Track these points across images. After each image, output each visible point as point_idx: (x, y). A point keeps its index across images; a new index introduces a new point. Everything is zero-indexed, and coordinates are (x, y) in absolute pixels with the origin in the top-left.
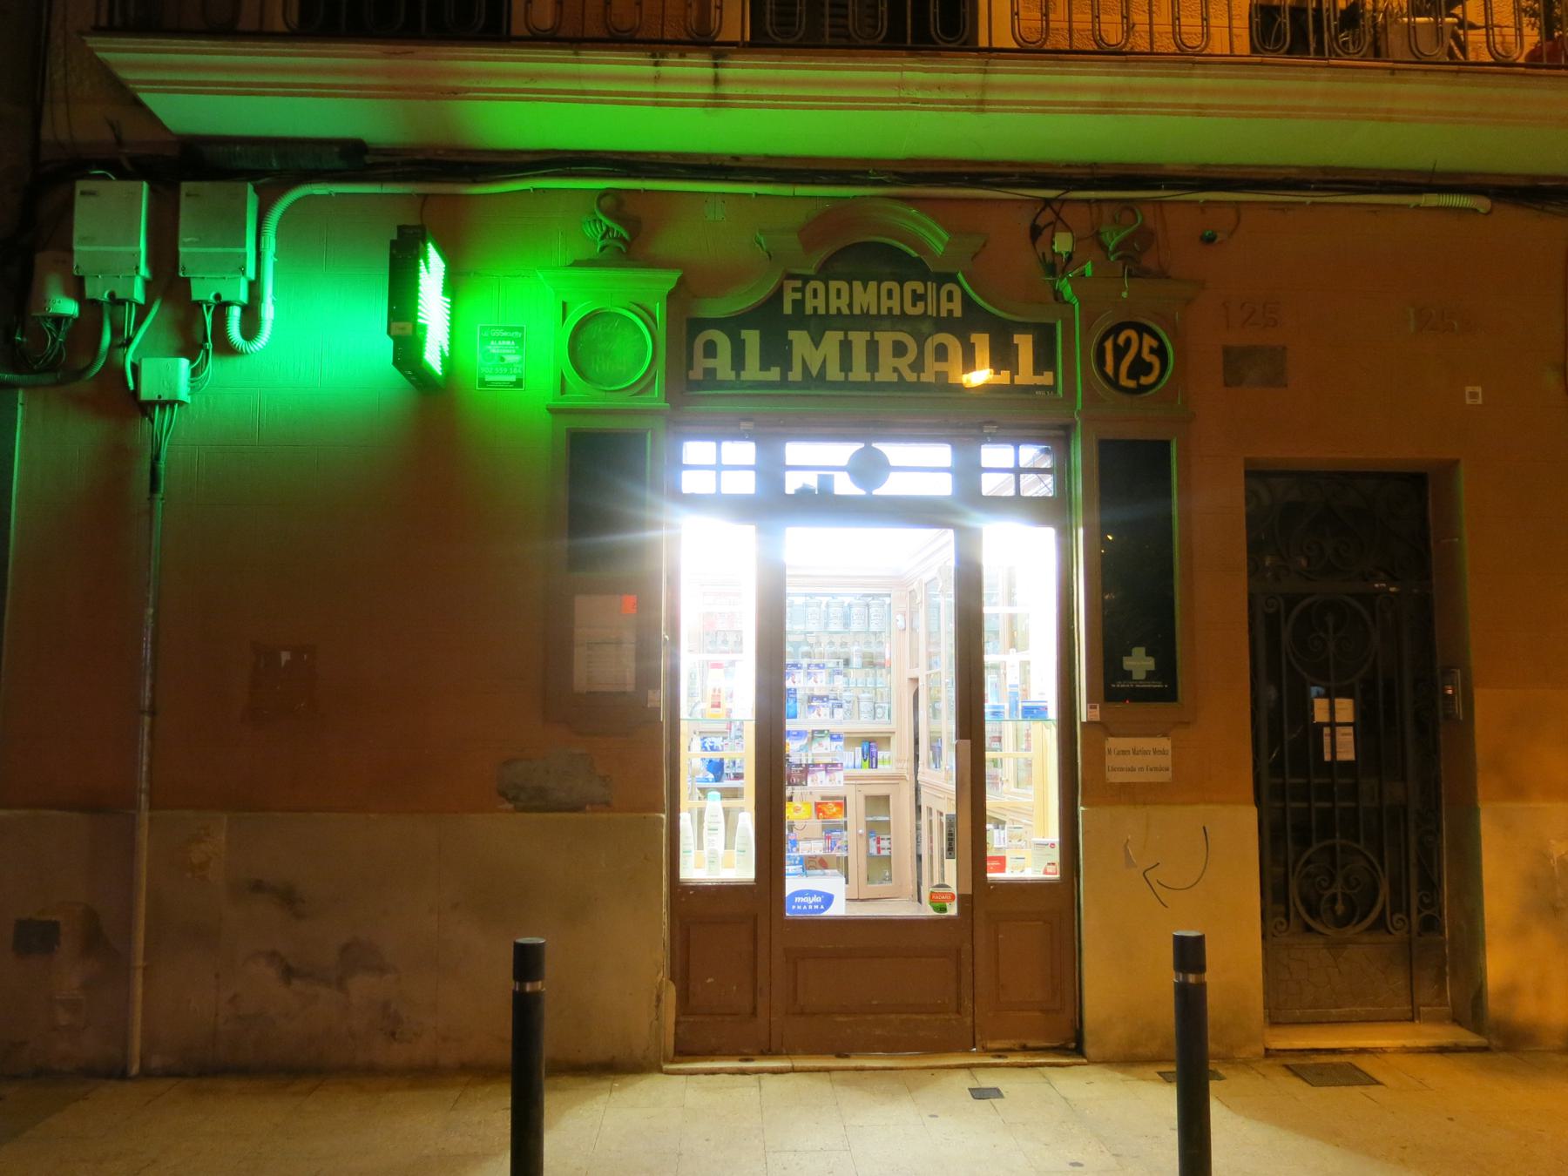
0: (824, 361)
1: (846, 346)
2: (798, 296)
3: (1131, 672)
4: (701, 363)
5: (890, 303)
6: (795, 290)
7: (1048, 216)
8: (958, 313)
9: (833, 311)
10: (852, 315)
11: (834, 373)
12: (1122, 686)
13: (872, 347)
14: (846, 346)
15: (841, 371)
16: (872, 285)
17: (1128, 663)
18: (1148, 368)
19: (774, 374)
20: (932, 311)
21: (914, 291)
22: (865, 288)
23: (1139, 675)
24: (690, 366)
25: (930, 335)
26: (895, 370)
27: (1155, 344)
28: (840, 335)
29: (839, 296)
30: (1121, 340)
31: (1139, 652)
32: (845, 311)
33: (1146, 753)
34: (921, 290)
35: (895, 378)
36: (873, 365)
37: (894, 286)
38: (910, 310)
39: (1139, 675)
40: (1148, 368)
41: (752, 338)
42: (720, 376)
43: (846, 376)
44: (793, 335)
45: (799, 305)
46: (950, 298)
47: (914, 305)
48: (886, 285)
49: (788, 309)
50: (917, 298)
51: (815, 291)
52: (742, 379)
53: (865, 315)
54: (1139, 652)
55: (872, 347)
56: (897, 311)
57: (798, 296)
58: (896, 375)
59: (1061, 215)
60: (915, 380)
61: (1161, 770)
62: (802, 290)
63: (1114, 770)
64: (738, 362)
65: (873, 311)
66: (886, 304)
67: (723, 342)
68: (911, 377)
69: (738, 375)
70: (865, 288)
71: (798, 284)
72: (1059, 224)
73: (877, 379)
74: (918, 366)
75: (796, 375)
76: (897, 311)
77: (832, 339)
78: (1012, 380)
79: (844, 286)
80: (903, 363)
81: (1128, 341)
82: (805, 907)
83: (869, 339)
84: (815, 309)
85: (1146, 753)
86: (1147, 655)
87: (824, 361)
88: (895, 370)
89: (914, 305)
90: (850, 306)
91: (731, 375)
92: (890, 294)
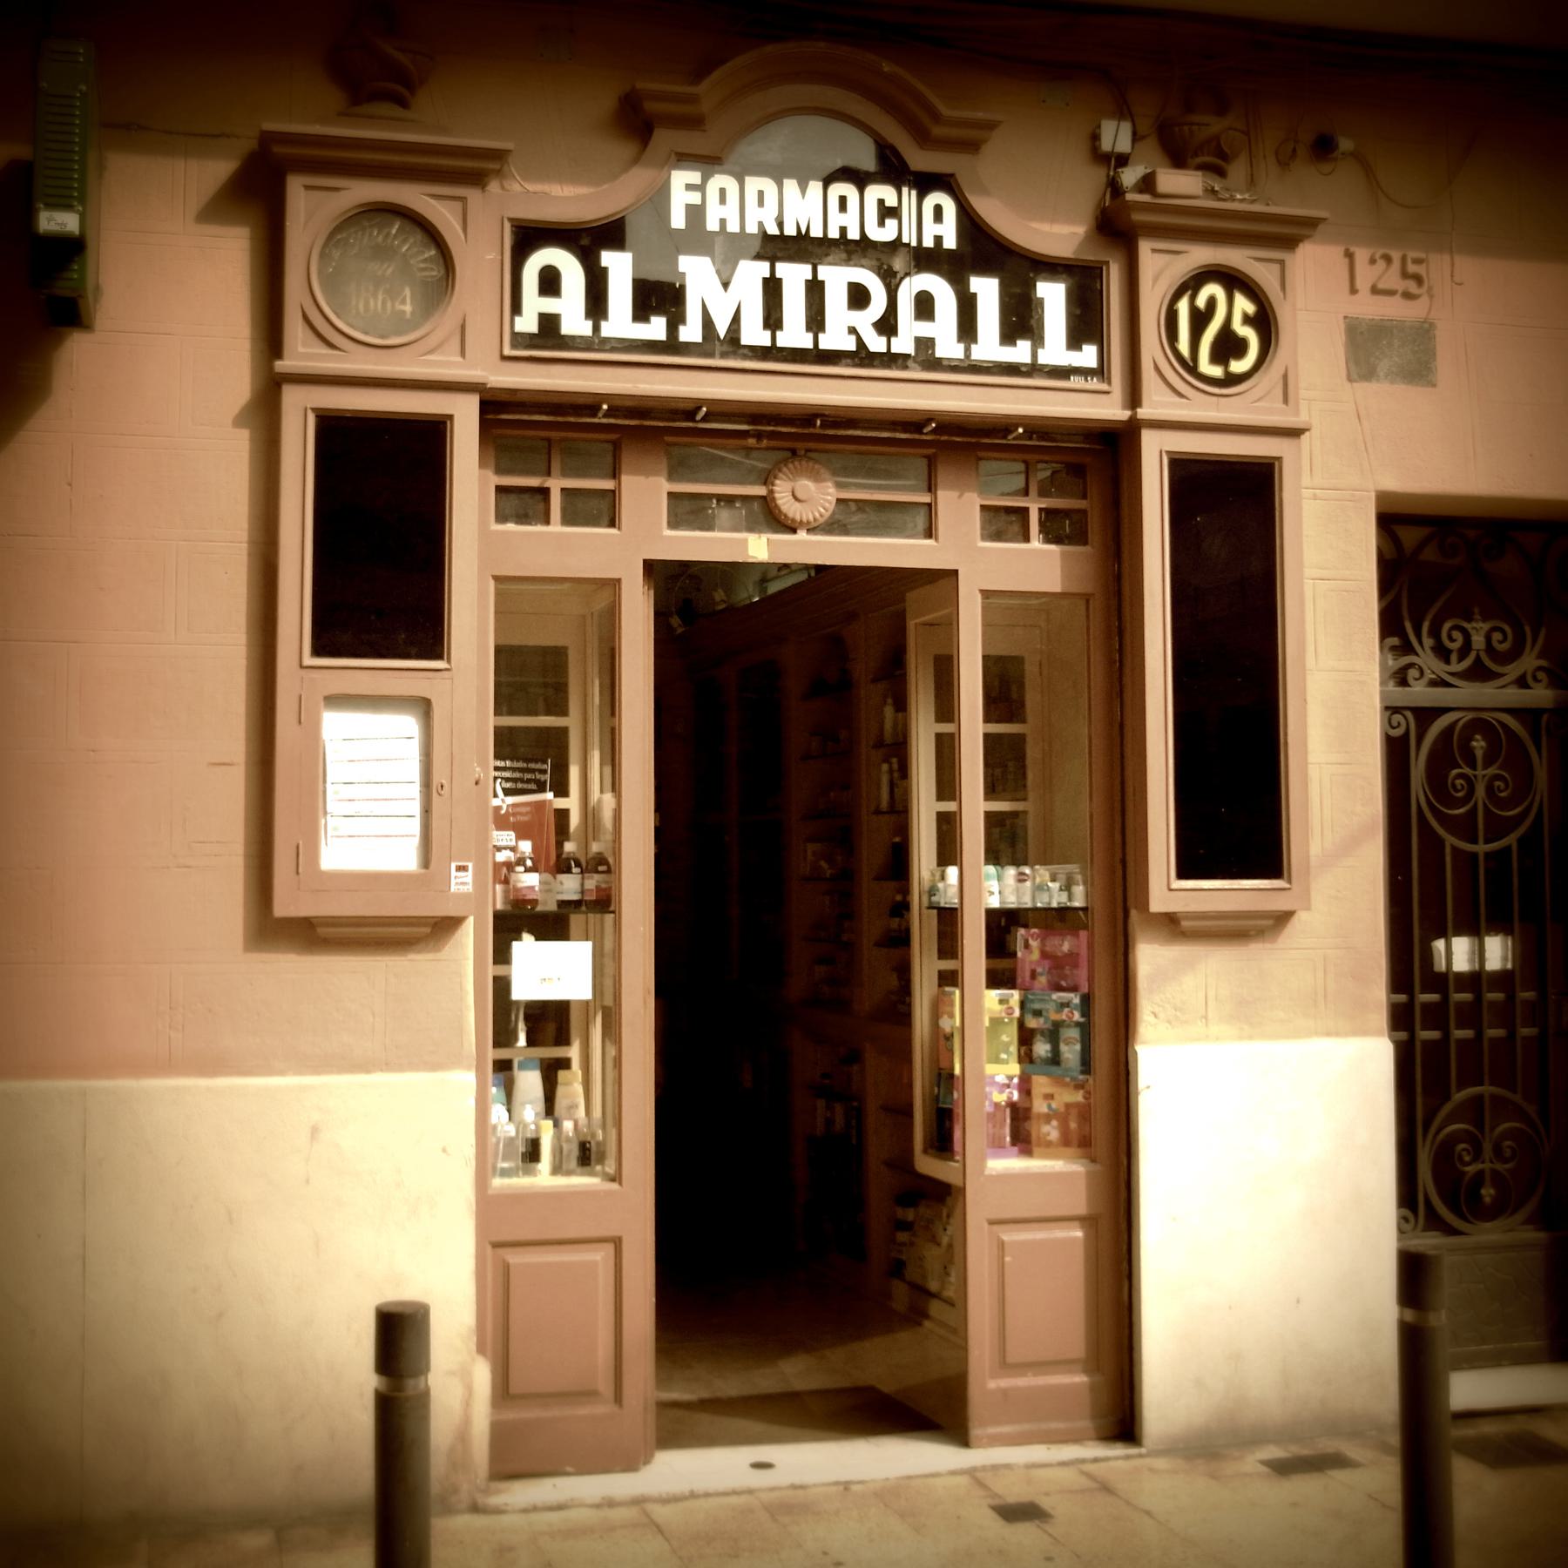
2: (695, 198)
4: (534, 304)
6: (689, 187)
8: (950, 243)
11: (754, 334)
13: (815, 290)
14: (772, 288)
18: (1239, 348)
19: (656, 328)
20: (909, 237)
21: (881, 202)
24: (516, 308)
25: (907, 274)
26: (852, 330)
27: (1251, 308)
28: (763, 268)
29: (761, 203)
30: (1201, 302)
34: (891, 198)
35: (850, 345)
36: (816, 321)
40: (1239, 348)
42: (566, 329)
45: (696, 214)
46: (938, 213)
47: (881, 223)
49: (678, 220)
50: (886, 212)
51: (723, 192)
55: (815, 290)
57: (695, 198)
58: (853, 338)
62: (701, 188)
65: (817, 232)
66: (836, 221)
68: (876, 344)
73: (822, 346)
74: (887, 325)
75: (691, 332)
78: (1034, 355)
79: (767, 185)
81: (1212, 302)
84: (723, 222)
88: (852, 330)
89: (881, 223)
91: (582, 327)
92: (843, 201)
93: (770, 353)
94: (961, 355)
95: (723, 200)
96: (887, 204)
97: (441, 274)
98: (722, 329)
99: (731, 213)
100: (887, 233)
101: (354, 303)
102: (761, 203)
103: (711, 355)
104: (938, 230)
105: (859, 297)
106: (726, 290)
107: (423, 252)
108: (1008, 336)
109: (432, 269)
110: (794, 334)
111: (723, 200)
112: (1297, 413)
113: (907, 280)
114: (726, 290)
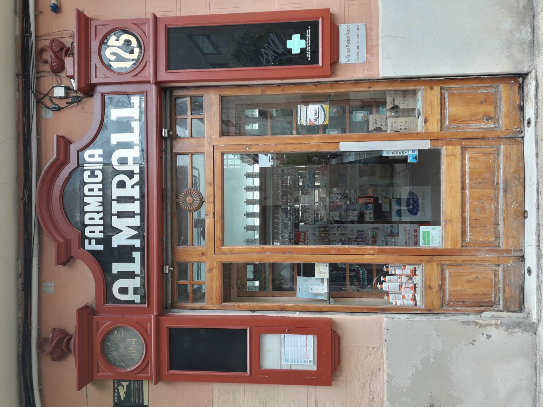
0: (129, 227)
1: (120, 215)
2: (93, 241)
3: (301, 49)
4: (130, 297)
5: (96, 190)
6: (90, 243)
7: (47, 101)
8: (100, 152)
9: (101, 222)
10: (103, 211)
12: (309, 53)
13: (120, 200)
14: (120, 215)
15: (134, 217)
16: (86, 200)
17: (296, 51)
18: (128, 42)
19: (136, 255)
21: (89, 176)
22: (88, 204)
23: (303, 44)
24: (133, 302)
25: (113, 167)
26: (133, 187)
28: (114, 218)
29: (93, 219)
30: (113, 58)
31: (290, 44)
32: (101, 215)
33: (348, 39)
34: (89, 173)
35: (137, 188)
36: (131, 199)
37: (87, 187)
38: (100, 179)
39: (303, 44)
40: (128, 42)
41: (117, 268)
43: (137, 214)
44: (115, 245)
45: (98, 241)
46: (92, 156)
47: (97, 176)
48: (87, 192)
49: (101, 247)
50: (93, 175)
51: (91, 232)
52: (139, 273)
53: (103, 204)
54: (290, 44)
55: (120, 200)
56: (100, 186)
57: (93, 241)
59: (46, 93)
60: (138, 175)
61: (358, 29)
62: (90, 239)
63: (358, 58)
64: (131, 275)
65: (101, 199)
66: (96, 192)
67: (119, 284)
68: (137, 178)
69: (137, 275)
70: (88, 204)
71: (87, 241)
72: (50, 95)
73: (139, 197)
74: (130, 174)
75: (137, 243)
76: (100, 186)
77: (116, 222)
79: (87, 216)
80: (129, 182)
81: (113, 54)
82: (415, 205)
83: (116, 202)
84: (100, 232)
85: (348, 39)
86: (291, 39)
87: (129, 227)
88: (133, 187)
89: (97, 176)
90: (98, 212)
91: (138, 279)
92: (91, 190)
93: (142, 214)
94: (138, 147)
95: (93, 232)
96: (90, 174)
97: (123, 329)
98: (135, 232)
99: (97, 229)
100: (99, 173)
101: (133, 357)
102: (93, 219)
103: (144, 236)
104: (96, 156)
105: (122, 185)
106: (122, 231)
107: (116, 335)
108: (130, 130)
109: (121, 332)
110: (135, 207)
111: (93, 232)
112: (149, 19)
113: (114, 167)
114: (122, 231)
